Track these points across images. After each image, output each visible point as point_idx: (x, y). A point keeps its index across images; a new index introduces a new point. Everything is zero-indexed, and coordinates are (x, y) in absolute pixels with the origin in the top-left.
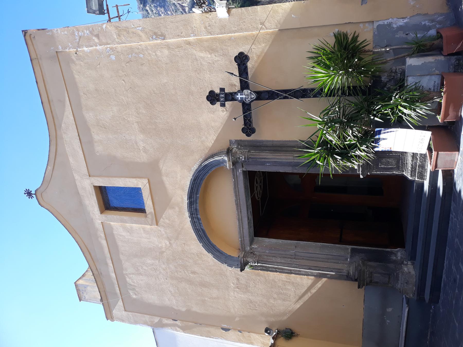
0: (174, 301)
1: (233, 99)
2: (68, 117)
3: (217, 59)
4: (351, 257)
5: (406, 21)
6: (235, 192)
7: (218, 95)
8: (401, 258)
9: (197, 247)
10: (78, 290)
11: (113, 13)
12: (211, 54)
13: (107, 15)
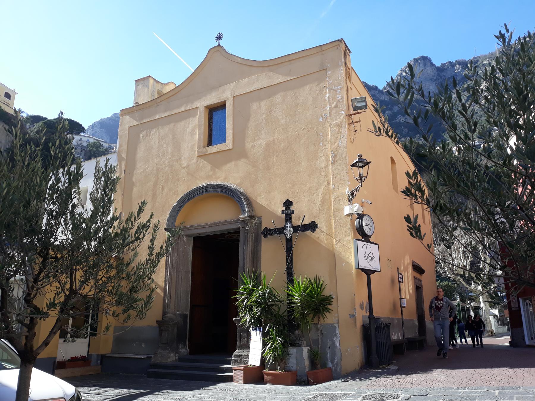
0: (139, 171)
1: (287, 220)
2: (278, 79)
3: (317, 206)
4: (180, 315)
5: (338, 346)
6: (224, 222)
7: (290, 208)
8: (180, 352)
9: (183, 190)
10: (144, 79)
11: (356, 118)
12: (321, 201)
13: (354, 112)
